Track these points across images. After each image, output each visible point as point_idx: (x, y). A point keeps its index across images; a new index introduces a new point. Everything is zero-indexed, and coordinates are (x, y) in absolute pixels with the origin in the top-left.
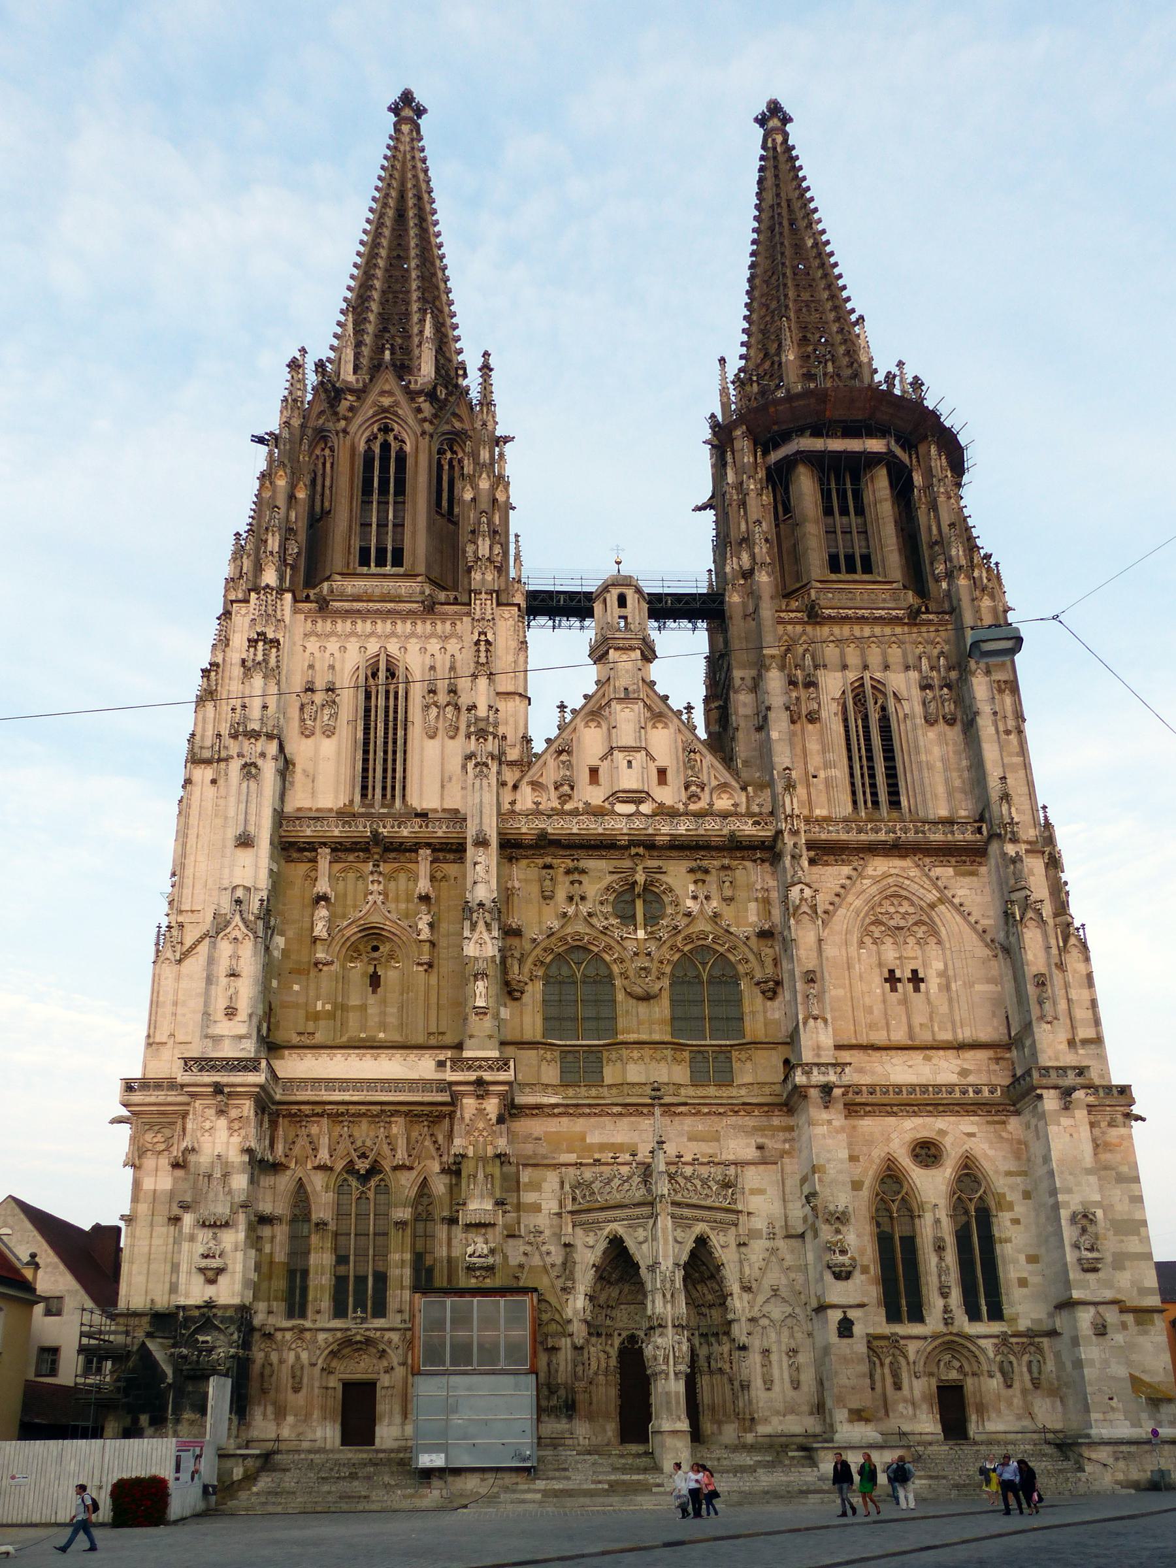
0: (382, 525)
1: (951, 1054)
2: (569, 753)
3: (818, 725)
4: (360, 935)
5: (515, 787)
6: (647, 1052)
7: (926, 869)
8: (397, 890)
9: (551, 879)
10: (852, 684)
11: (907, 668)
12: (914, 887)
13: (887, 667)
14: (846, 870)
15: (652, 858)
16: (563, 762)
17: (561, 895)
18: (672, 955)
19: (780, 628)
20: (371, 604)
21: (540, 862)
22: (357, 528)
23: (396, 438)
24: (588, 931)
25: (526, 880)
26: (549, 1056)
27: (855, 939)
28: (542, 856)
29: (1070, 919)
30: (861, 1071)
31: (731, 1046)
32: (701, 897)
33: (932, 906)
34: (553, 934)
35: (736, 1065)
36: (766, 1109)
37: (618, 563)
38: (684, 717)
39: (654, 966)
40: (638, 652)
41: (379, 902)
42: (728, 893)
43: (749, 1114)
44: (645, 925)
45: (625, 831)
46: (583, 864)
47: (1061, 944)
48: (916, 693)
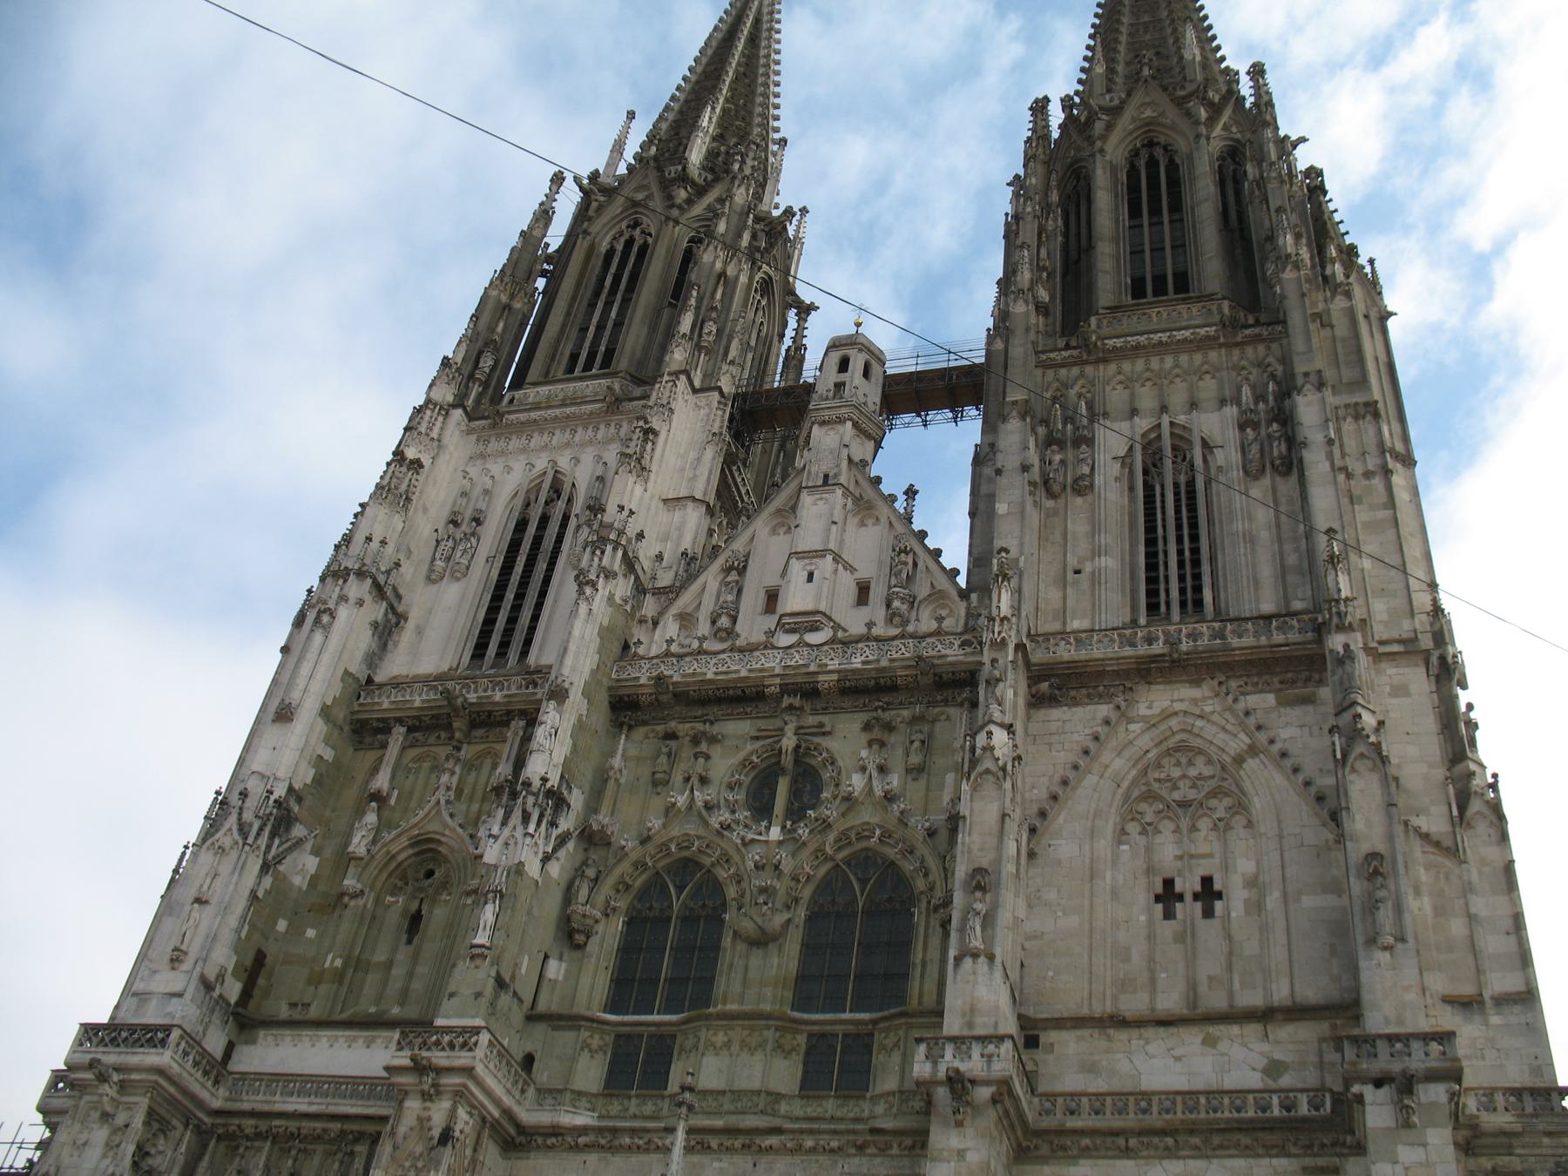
0: (600, 327)
1: (1253, 1029)
2: (742, 571)
3: (1089, 498)
4: (410, 851)
5: (655, 623)
6: (738, 1033)
7: (1230, 698)
8: (476, 782)
9: (669, 755)
10: (1144, 435)
11: (1223, 402)
12: (1209, 731)
13: (1193, 405)
14: (1104, 710)
15: (815, 712)
16: (727, 584)
17: (677, 778)
18: (817, 867)
19: (1050, 374)
20: (549, 412)
21: (660, 728)
22: (574, 334)
23: (643, 232)
24: (701, 832)
25: (638, 759)
26: (596, 1042)
27: (1108, 827)
28: (664, 720)
29: (1473, 767)
30: (1091, 1068)
31: (875, 1022)
32: (872, 768)
33: (1239, 760)
34: (649, 838)
35: (878, 1058)
36: (908, 1141)
37: (858, 325)
38: (900, 505)
39: (781, 886)
40: (849, 424)
41: (443, 802)
42: (915, 759)
43: (883, 1150)
44: (786, 818)
45: (777, 672)
46: (715, 729)
47: (1455, 812)
48: (1233, 435)
